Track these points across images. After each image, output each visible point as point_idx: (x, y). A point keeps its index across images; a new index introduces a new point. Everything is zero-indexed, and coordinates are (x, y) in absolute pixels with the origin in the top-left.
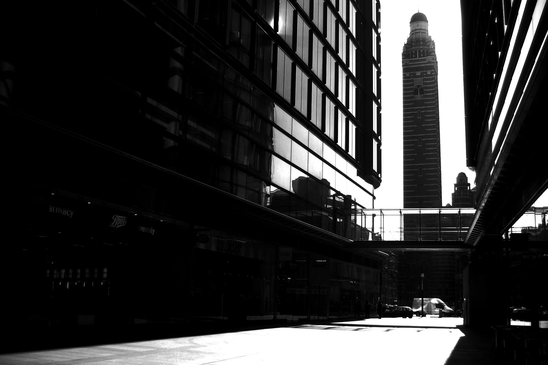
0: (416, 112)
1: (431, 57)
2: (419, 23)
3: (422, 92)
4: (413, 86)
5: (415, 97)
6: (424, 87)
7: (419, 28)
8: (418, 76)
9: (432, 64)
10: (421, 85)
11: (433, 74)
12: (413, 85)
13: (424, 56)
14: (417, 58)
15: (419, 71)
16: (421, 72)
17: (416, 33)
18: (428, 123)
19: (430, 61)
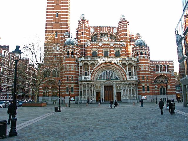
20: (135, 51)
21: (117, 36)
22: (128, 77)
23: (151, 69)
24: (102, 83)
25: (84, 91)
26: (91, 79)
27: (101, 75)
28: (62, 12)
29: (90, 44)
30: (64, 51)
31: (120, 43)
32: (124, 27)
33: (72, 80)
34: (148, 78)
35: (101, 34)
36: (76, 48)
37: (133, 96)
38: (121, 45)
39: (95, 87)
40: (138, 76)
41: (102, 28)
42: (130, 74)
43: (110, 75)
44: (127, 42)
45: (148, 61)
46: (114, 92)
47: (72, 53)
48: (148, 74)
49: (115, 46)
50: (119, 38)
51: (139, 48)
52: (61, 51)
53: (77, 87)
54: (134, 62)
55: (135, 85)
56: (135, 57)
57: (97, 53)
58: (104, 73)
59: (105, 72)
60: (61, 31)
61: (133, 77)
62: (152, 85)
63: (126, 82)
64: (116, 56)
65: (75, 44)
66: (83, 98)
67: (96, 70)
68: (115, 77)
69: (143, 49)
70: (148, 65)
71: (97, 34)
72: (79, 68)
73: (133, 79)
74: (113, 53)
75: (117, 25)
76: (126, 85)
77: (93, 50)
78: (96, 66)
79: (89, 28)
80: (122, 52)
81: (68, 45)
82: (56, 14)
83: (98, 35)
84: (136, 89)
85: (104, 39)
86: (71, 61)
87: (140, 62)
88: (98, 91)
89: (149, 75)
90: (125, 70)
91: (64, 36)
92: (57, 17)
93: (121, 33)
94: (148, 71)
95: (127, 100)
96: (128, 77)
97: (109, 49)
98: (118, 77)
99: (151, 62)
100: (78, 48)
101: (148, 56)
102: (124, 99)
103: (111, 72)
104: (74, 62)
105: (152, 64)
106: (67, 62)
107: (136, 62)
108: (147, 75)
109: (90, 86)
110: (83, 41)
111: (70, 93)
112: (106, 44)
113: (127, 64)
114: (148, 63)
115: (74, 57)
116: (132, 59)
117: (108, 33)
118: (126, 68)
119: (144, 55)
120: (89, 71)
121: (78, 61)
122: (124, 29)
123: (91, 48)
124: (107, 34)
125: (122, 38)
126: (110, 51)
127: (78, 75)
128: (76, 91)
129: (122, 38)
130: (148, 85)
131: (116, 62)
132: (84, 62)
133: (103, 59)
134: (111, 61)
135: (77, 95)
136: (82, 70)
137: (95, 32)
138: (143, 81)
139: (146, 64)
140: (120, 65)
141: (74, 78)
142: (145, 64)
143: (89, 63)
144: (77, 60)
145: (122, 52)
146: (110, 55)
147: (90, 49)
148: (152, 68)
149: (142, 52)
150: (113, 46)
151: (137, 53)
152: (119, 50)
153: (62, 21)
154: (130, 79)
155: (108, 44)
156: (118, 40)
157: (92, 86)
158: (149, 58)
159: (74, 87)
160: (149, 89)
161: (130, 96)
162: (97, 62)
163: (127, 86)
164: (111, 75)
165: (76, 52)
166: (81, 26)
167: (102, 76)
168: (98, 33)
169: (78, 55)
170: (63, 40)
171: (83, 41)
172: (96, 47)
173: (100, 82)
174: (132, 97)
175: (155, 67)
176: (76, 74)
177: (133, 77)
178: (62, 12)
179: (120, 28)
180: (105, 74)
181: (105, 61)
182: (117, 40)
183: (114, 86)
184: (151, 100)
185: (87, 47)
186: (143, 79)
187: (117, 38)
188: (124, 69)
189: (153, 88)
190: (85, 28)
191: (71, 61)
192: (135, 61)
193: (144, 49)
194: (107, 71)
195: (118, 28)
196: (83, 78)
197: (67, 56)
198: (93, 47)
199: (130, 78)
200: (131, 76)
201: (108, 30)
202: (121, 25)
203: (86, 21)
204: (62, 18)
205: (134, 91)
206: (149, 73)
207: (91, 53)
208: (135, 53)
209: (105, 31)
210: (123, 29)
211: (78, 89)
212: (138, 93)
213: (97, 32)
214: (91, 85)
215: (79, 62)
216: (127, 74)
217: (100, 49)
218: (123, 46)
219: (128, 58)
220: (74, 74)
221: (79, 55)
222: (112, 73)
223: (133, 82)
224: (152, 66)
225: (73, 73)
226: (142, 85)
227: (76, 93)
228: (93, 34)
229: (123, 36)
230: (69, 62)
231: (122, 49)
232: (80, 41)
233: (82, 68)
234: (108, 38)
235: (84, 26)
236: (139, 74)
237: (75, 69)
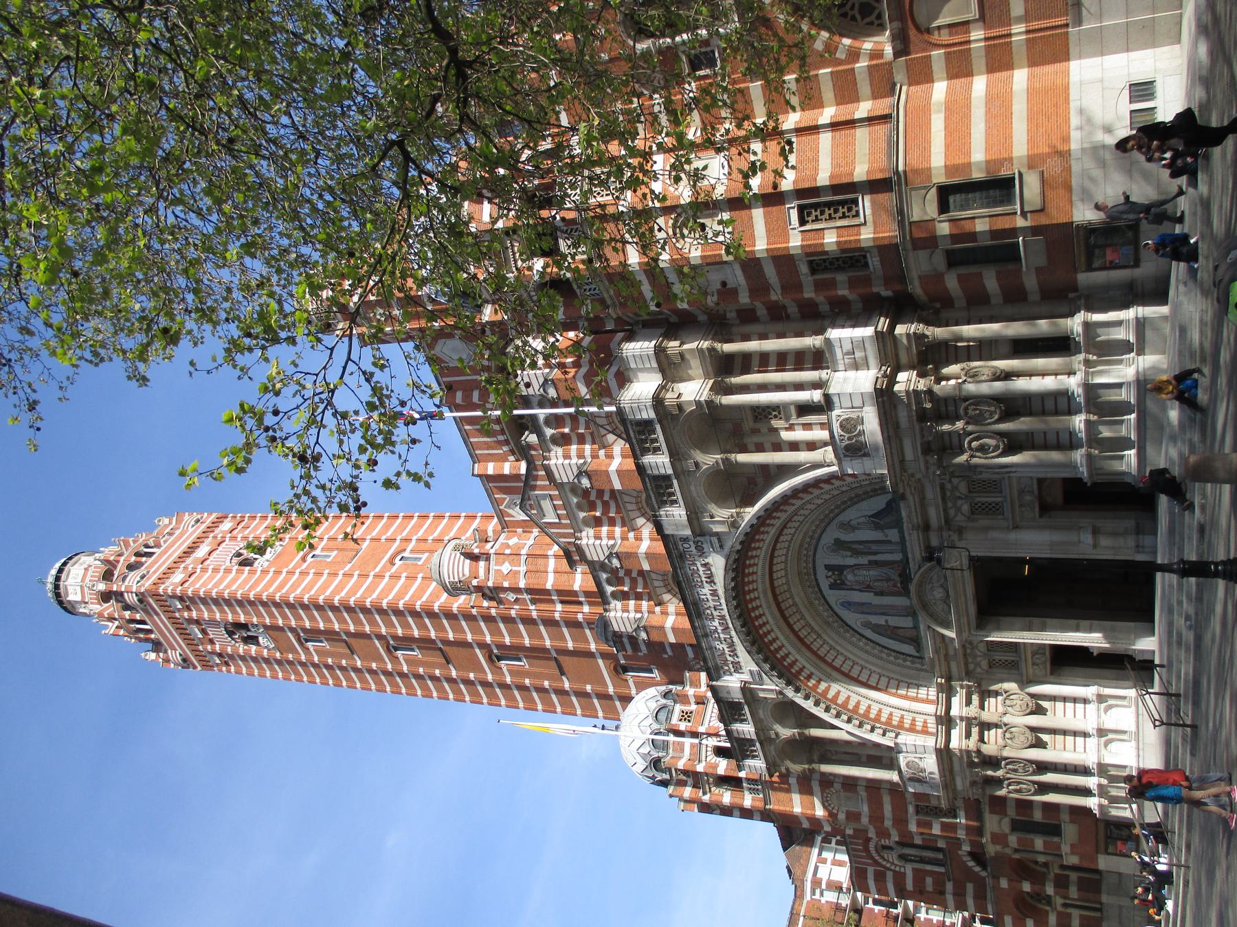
27: (876, 629)
43: (863, 560)
58: (848, 605)
59: (833, 596)
68: (877, 527)
98: (864, 505)
103: (825, 558)
111: (1065, 849)
134: (721, 592)
164: (856, 553)
167: (875, 619)
180: (857, 597)
181: (733, 633)
183: (981, 550)
194: (824, 584)
222: (839, 545)
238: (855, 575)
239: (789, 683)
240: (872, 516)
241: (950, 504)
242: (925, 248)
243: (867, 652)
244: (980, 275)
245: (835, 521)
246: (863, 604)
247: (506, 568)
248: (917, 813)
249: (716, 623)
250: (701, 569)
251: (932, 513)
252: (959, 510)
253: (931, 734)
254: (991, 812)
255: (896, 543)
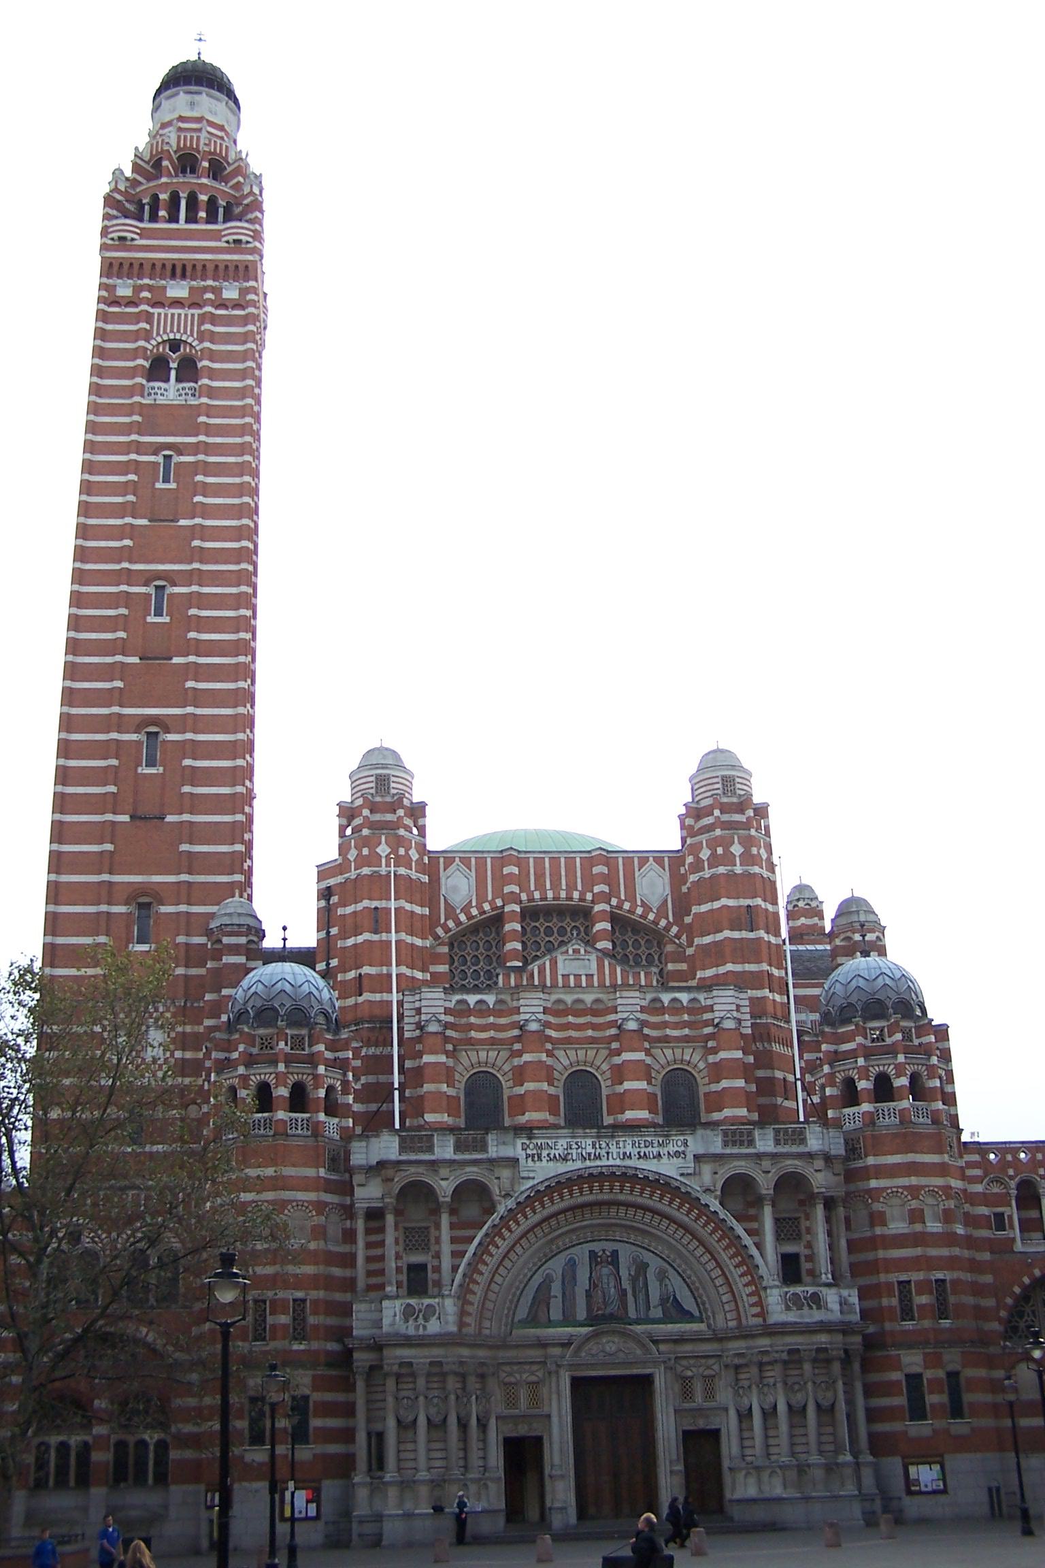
0: (152, 458)
1: (246, 225)
2: (200, 93)
3: (189, 370)
4: (148, 341)
5: (153, 388)
6: (201, 350)
7: (195, 114)
8: (177, 303)
9: (250, 258)
10: (185, 342)
11: (251, 297)
12: (147, 336)
13: (212, 219)
14: (177, 221)
15: (184, 276)
16: (194, 283)
17: (180, 129)
18: (206, 511)
19: (239, 241)
20: (826, 1069)
21: (675, 929)
22: (774, 1298)
23: (970, 1221)
24: (557, 1351)
25: (406, 1426)
26: (461, 1324)
28: (196, 723)
29: (447, 1011)
30: (230, 1079)
31: (701, 997)
32: (728, 859)
33: (299, 1331)
34: (952, 1299)
35: (530, 914)
36: (328, 1055)
37: (831, 1468)
38: (707, 1016)
39: (498, 1395)
40: (864, 1281)
41: (539, 862)
42: (791, 1269)
43: (626, 1285)
44: (756, 980)
45: (941, 1153)
46: (659, 1434)
47: (299, 1099)
48: (951, 1263)
49: (655, 1026)
50: (690, 951)
51: (859, 1039)
52: (184, 1068)
53: (340, 1397)
54: (819, 1163)
55: (836, 1367)
56: (825, 1122)
57: (509, 1089)
58: (572, 1264)
60: (187, 893)
61: (816, 1300)
62: (990, 1363)
63: (764, 1342)
64: (666, 1111)
65: (321, 1020)
66: (392, 1492)
67: (503, 1245)
68: (663, 1301)
69: (892, 1051)
70: (947, 1189)
71: (498, 919)
72: (360, 1224)
73: (817, 1316)
74: (642, 1085)
75: (671, 840)
76: (761, 1365)
77: (469, 1060)
78: (501, 1210)
79: (434, 863)
80: (717, 1071)
81: (261, 1031)
82: (144, 738)
83: (508, 927)
84: (850, 1402)
85: (560, 972)
86: (289, 1171)
87: (871, 1160)
88: (522, 1430)
89: (956, 1275)
90: (750, 1232)
91: (208, 933)
92: (152, 771)
93: (704, 908)
94: (949, 1239)
95: (779, 1500)
96: (774, 1298)
97: (604, 1053)
99: (967, 1158)
100: (341, 1055)
101: (939, 1105)
102: (752, 1492)
103: (626, 1254)
104: (310, 1172)
105: (977, 1172)
106: (252, 1172)
107: (839, 1167)
108: (940, 1275)
109: (452, 1383)
110: (383, 983)
112: (577, 1014)
113: (765, 1184)
114: (942, 1170)
115: (316, 1130)
116: (803, 1141)
117: (597, 908)
118: (755, 1218)
119: (907, 1103)
120: (446, 1248)
121: (350, 1170)
122: (731, 876)
123: (450, 1047)
124: (582, 914)
125: (716, 954)
126: (619, 1074)
127: (349, 1285)
128: (328, 1436)
129: (716, 954)
130: (952, 1358)
131: (668, 1168)
132: (400, 1180)
133: (562, 1143)
134: (628, 1163)
135: (343, 1467)
136: (382, 1244)
137: (481, 898)
138: (909, 1325)
139: (923, 1181)
140: (705, 1199)
141: (315, 1312)
142: (914, 1181)
143: (445, 1187)
144: (339, 1160)
145: (717, 1071)
146: (620, 1102)
147: (442, 1058)
148: (984, 1210)
149: (891, 1071)
150: (644, 1024)
151: (850, 1084)
152: (692, 1057)
153: (196, 804)
154: (791, 1317)
155: (595, 1013)
156: (684, 966)
157: (472, 1380)
158: (954, 1120)
159: (316, 1397)
160: (968, 1398)
161: (802, 1469)
162: (506, 1173)
163: (774, 1373)
164: (634, 1280)
165: (330, 1089)
166: (365, 851)
167: (556, 1289)
168: (507, 909)
169: (344, 1111)
170: (202, 971)
171: (383, 983)
172: (493, 1042)
173: (542, 1344)
174: (819, 1473)
175: (1003, 1200)
176: (328, 1283)
177: (816, 1300)
178: (196, 723)
179: (697, 866)
180: (583, 1275)
181: (579, 1164)
182: (670, 966)
184: (984, 1497)
185: (419, 1040)
186: (907, 1312)
187: (669, 948)
188: (740, 1230)
189: (995, 1386)
190: (402, 871)
191: (289, 1171)
192: (828, 1158)
193: (907, 1051)
194: (596, 1247)
195: (672, 862)
196: (392, 1314)
197: (257, 1124)
198: (471, 1042)
199: (795, 1302)
200: (798, 1289)
201: (590, 881)
202: (703, 838)
203: (401, 812)
204: (195, 776)
205: (833, 1424)
206: (956, 1251)
207: (451, 1092)
208: (833, 1085)
209: (571, 887)
210: (722, 870)
211: (348, 1410)
212: (872, 1436)
213: (499, 903)
214: (463, 1377)
215: (358, 1179)
216: (763, 1270)
217: (527, 1057)
218: (728, 1024)
219: (770, 1133)
220: (314, 1282)
221: (357, 1107)
222: (642, 1267)
223: (823, 1338)
224: (979, 1188)
225: (309, 1269)
226: (896, 1365)
227: (333, 1449)
228: (463, 917)
229: (719, 937)
230: (270, 1171)
231: (714, 1051)
232: (359, 985)
233: (382, 1230)
234: (593, 957)
235: (383, 850)
236: (873, 1267)
237: (319, 1232)
238: (608, 1276)
239: (519, 1203)
240: (674, 1296)
241: (692, 1362)
242: (925, 1361)
243: (518, 1275)
244: (900, 1394)
245: (668, 1266)
246: (574, 1278)
247: (414, 855)
248: (295, 1300)
249: (590, 1149)
250: (655, 1151)
251: (688, 1347)
252: (687, 1368)
253: (460, 1330)
254: (314, 1377)
255: (647, 1315)
